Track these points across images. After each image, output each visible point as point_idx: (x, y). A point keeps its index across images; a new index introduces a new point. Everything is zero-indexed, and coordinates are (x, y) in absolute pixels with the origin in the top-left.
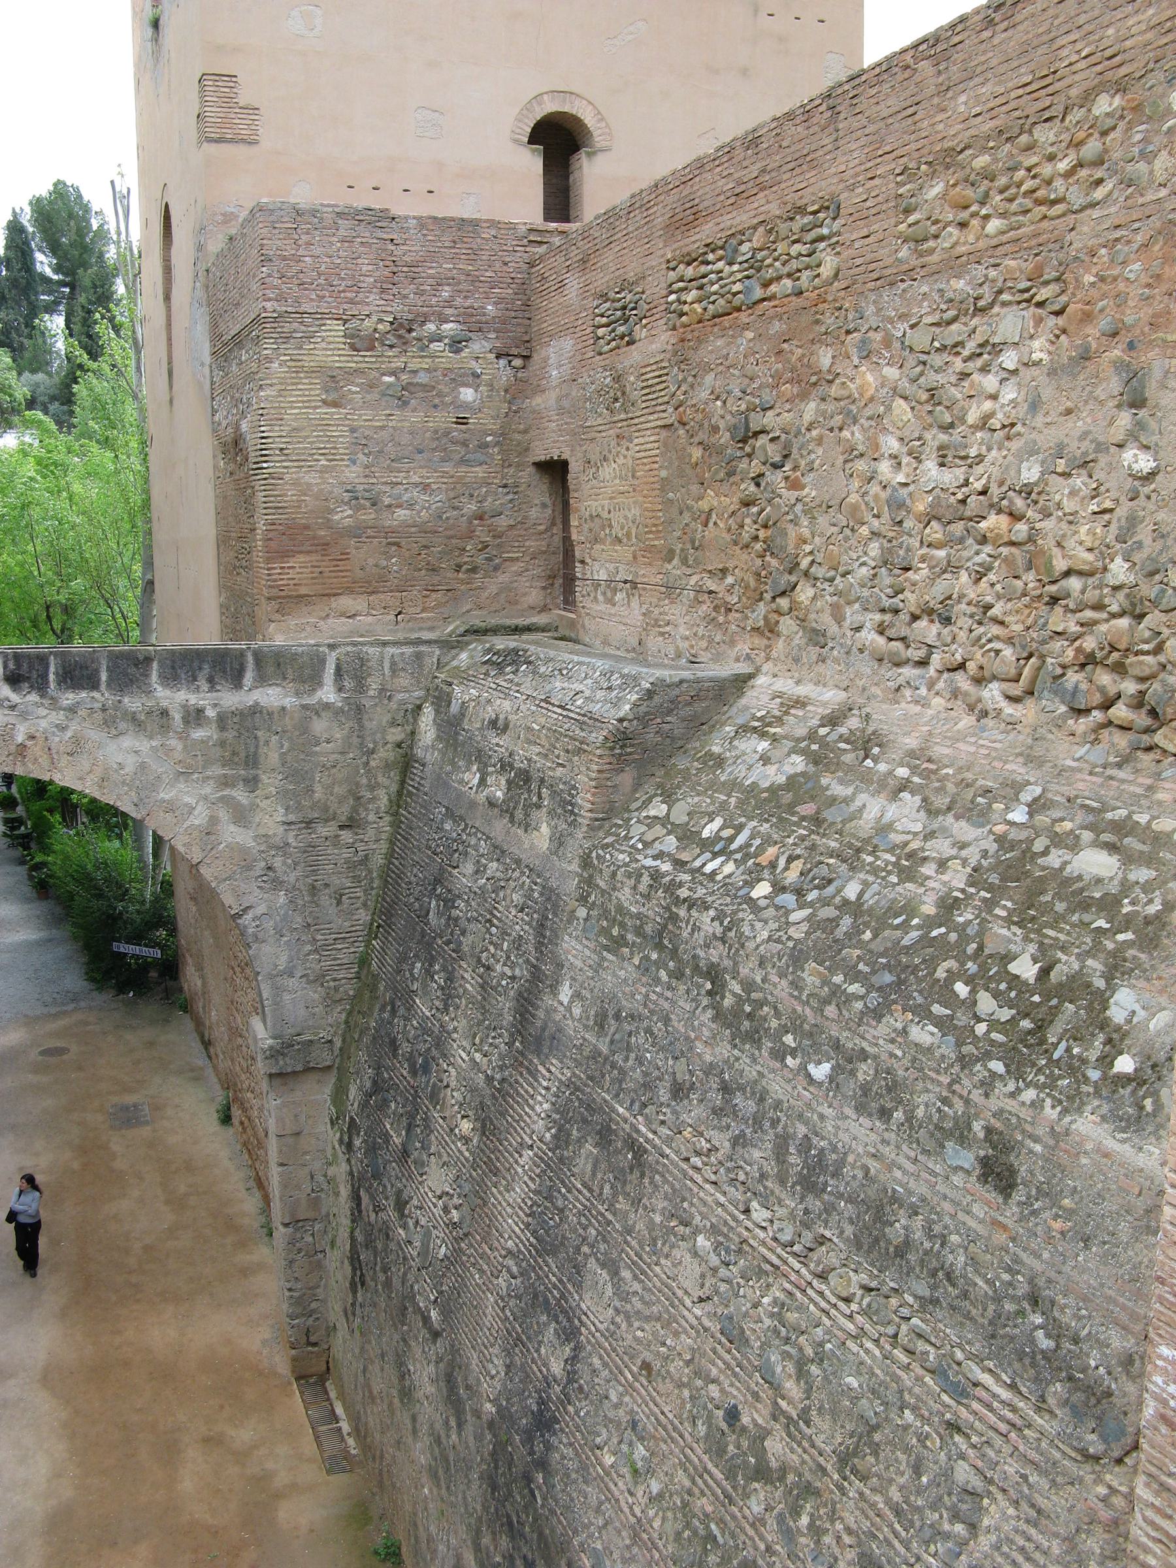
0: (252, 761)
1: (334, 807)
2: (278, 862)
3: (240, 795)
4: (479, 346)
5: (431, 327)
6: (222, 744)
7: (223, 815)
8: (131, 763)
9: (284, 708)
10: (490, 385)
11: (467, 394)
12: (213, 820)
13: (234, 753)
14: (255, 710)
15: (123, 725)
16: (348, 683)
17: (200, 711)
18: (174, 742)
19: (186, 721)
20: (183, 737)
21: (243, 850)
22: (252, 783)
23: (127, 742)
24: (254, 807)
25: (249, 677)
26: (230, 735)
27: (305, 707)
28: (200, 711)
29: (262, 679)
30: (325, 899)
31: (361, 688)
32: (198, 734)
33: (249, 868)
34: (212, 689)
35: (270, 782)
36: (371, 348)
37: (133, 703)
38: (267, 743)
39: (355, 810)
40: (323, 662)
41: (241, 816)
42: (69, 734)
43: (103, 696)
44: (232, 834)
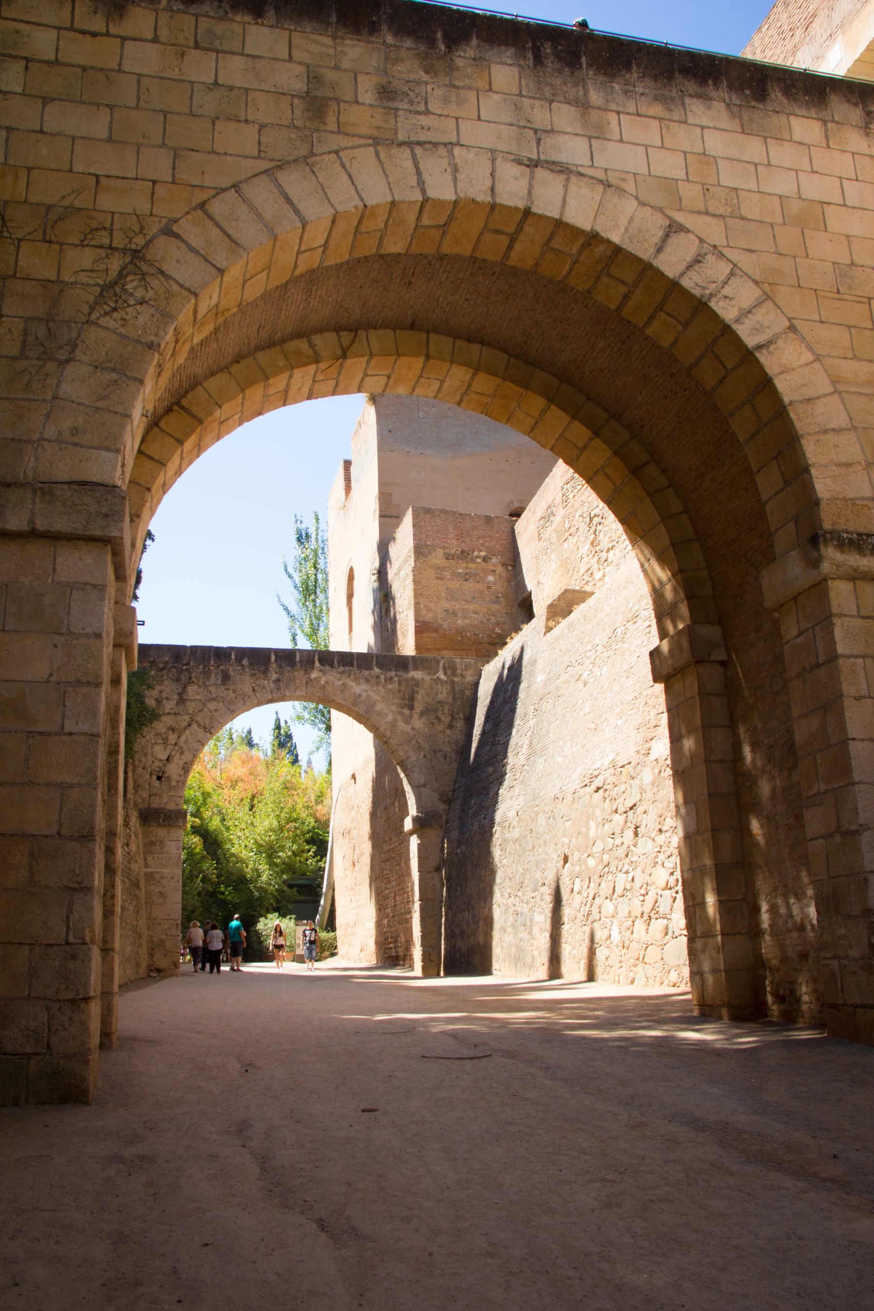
0: (412, 698)
1: (443, 718)
2: (421, 741)
3: (406, 711)
4: (494, 560)
5: (476, 553)
6: (400, 691)
7: (399, 718)
8: (364, 695)
9: (423, 679)
10: (500, 575)
11: (491, 578)
12: (395, 720)
13: (404, 695)
14: (412, 679)
15: (361, 681)
16: (449, 672)
17: (391, 678)
18: (380, 688)
19: (386, 680)
20: (384, 686)
21: (407, 733)
22: (411, 707)
23: (364, 686)
24: (411, 717)
25: (410, 667)
26: (403, 688)
27: (432, 679)
28: (391, 678)
29: (416, 669)
30: (439, 755)
31: (454, 674)
32: (390, 687)
33: (410, 741)
34: (396, 670)
35: (419, 707)
36: (453, 559)
37: (366, 673)
38: (417, 692)
39: (451, 721)
40: (438, 662)
41: (407, 720)
42: (341, 682)
43: (355, 669)
44: (401, 725)
